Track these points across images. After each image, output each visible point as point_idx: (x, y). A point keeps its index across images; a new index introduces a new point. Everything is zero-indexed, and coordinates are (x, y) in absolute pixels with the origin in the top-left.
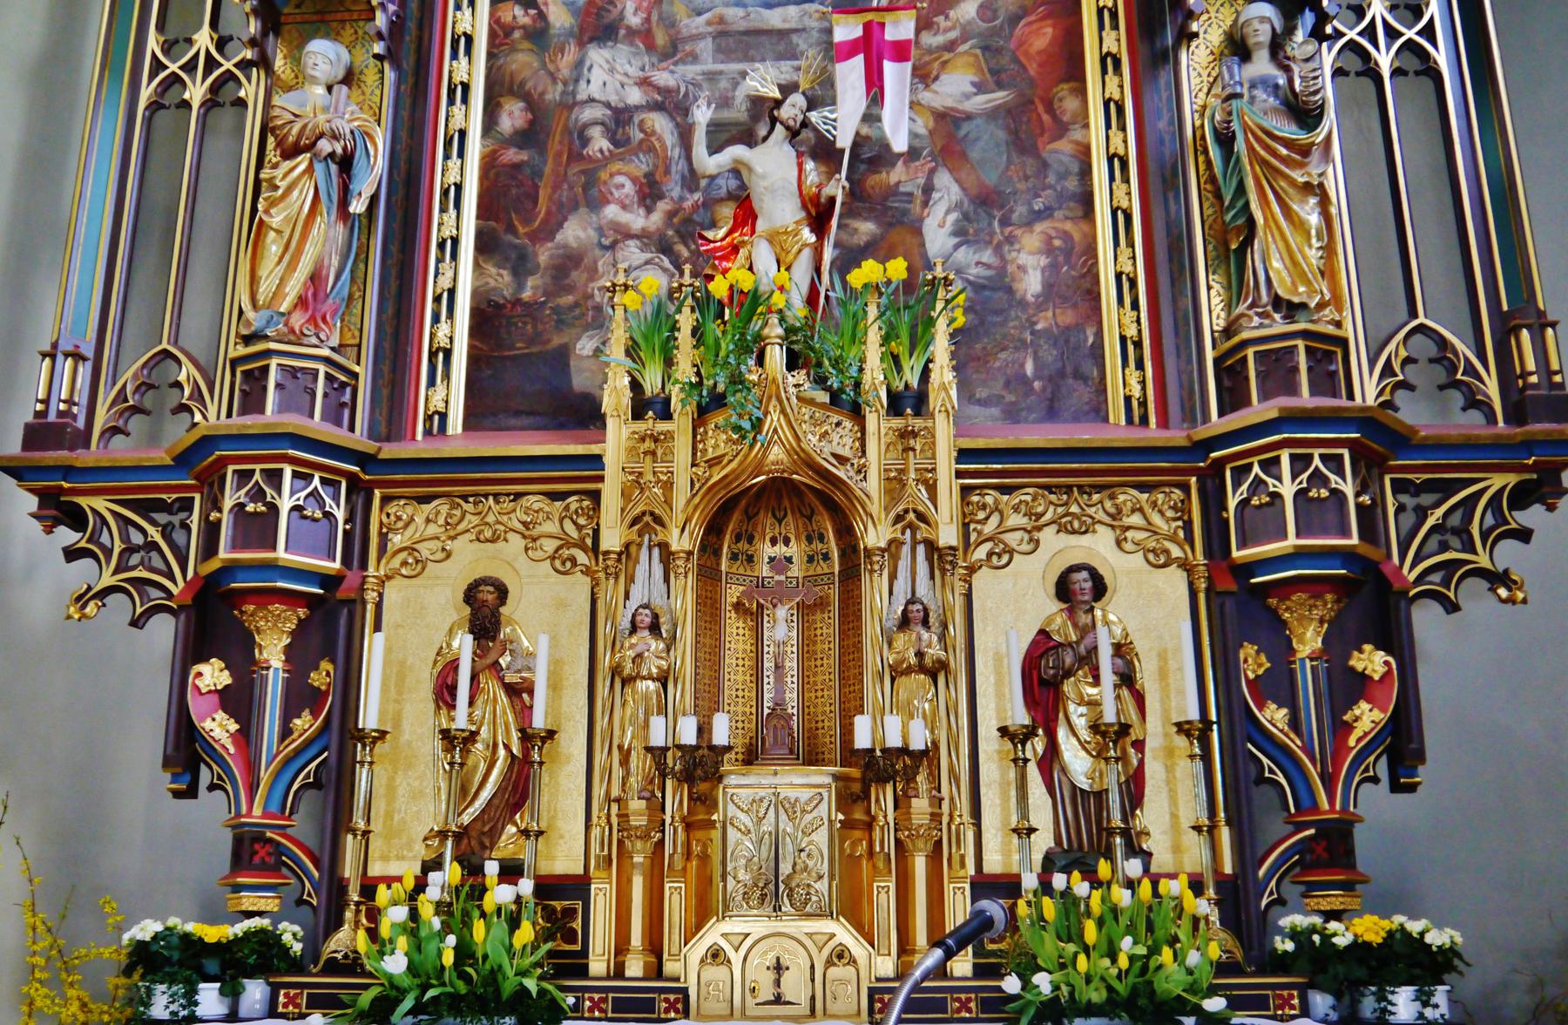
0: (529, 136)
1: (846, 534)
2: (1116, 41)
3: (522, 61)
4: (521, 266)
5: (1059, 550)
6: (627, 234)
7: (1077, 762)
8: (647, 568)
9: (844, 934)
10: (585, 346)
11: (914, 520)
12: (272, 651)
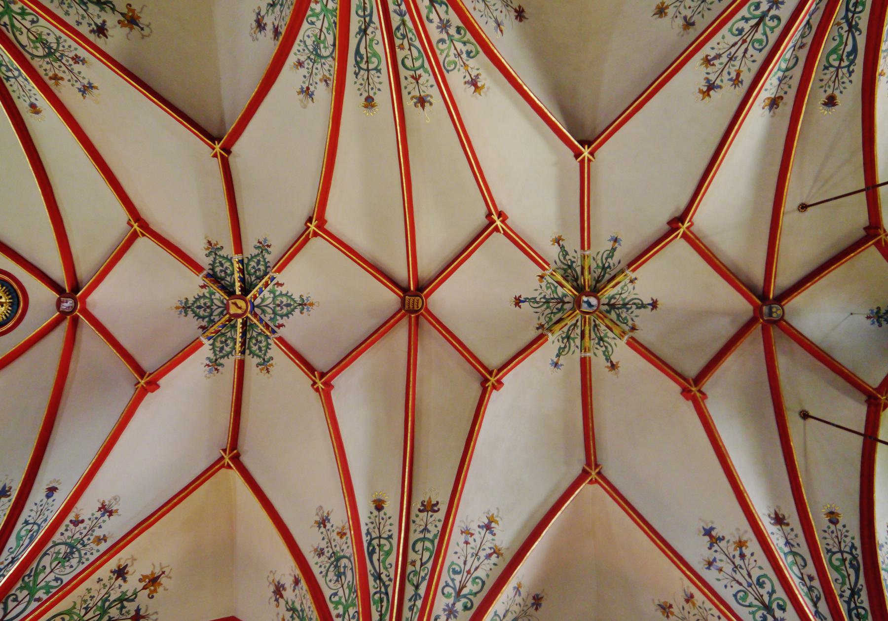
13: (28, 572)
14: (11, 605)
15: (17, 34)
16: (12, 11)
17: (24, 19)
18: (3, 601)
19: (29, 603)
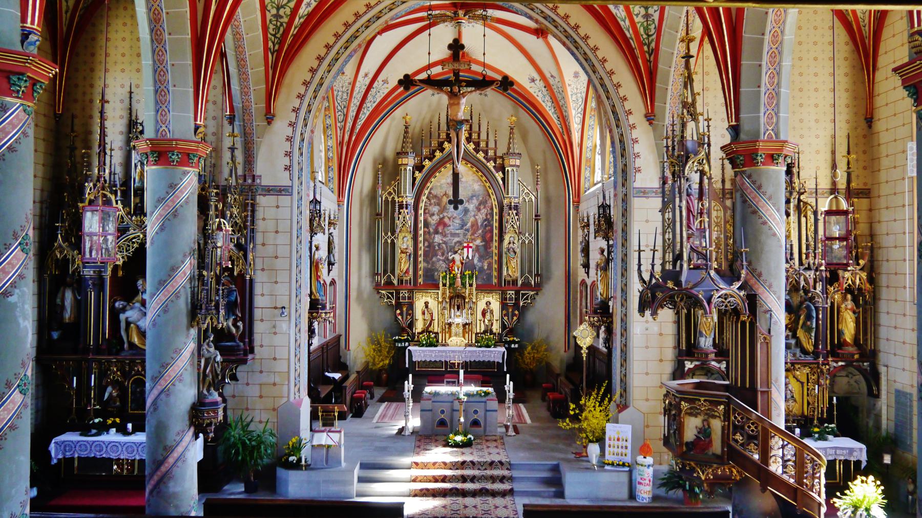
0: (429, 246)
2: (497, 239)
5: (486, 299)
6: (440, 260)
7: (486, 321)
8: (444, 303)
9: (463, 339)
10: (436, 274)
11: (471, 299)
12: (405, 309)
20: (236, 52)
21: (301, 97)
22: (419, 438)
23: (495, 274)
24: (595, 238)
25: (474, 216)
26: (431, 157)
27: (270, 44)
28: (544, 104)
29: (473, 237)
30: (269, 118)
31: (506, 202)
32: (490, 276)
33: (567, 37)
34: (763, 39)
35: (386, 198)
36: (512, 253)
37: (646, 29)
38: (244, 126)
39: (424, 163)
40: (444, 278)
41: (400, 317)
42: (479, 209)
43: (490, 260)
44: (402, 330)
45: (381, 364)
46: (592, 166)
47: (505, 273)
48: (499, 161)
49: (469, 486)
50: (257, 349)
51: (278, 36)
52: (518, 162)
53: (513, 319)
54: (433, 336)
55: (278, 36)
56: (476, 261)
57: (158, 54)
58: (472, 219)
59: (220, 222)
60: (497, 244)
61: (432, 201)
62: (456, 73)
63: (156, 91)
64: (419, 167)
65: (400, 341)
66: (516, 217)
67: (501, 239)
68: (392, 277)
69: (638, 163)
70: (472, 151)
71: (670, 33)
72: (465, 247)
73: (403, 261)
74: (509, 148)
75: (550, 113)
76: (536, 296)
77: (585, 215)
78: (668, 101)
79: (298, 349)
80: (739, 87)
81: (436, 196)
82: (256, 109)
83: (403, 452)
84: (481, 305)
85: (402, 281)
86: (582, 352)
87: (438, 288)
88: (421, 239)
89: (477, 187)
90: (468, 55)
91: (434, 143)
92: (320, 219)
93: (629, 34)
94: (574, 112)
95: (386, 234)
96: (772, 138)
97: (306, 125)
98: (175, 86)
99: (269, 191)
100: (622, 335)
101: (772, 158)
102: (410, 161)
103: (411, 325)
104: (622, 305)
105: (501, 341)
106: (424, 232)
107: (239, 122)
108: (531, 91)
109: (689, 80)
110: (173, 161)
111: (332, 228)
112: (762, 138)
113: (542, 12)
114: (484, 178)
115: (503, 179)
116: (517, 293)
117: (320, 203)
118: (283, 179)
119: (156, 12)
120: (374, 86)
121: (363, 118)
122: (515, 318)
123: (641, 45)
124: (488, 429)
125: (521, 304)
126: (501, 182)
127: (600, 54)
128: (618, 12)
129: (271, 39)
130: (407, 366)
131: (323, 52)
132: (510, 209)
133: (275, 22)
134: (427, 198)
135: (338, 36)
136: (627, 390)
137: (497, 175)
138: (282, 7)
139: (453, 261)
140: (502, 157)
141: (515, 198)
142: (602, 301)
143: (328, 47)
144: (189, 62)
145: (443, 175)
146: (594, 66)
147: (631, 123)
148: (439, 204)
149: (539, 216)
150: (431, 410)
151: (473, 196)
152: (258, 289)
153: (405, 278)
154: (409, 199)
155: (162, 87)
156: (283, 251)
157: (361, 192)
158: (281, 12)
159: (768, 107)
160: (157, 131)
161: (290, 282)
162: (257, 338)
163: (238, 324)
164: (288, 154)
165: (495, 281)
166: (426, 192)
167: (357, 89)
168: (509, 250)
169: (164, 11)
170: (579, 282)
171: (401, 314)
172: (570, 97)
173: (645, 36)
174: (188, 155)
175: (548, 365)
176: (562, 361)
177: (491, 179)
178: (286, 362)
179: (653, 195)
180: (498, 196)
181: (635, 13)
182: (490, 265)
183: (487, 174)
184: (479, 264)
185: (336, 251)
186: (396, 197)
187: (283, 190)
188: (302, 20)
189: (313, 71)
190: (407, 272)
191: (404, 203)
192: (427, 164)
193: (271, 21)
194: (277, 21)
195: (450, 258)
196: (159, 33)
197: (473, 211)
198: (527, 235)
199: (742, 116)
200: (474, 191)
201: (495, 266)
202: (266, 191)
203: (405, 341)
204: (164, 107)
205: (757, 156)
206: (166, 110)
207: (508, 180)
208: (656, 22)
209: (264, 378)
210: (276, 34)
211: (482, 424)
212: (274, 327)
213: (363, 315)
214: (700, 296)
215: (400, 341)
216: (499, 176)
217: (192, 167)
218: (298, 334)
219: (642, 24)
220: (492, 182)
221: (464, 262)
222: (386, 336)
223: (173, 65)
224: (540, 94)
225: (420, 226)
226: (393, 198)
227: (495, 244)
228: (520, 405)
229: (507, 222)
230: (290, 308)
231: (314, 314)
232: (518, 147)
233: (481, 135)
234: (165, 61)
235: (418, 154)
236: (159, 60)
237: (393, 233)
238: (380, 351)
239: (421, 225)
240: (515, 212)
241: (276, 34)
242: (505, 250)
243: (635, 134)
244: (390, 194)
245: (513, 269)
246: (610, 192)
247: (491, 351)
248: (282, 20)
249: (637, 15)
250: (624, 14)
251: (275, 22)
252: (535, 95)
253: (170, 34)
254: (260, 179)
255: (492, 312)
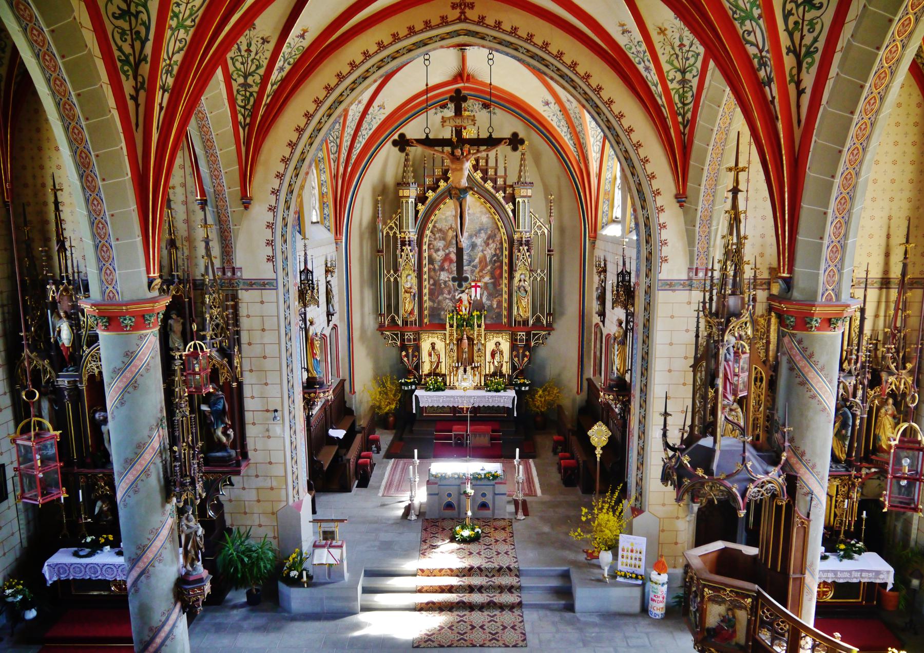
0: (434, 284)
1: (473, 342)
2: (506, 275)
3: (432, 273)
4: (433, 301)
5: (496, 340)
7: (496, 363)
8: (451, 344)
10: (442, 313)
12: (410, 351)
13: (730, 13)
14: (751, 38)
15: (195, 9)
16: (178, 22)
17: (180, 12)
18: (744, 42)
19: (758, 24)
20: (200, 132)
21: (280, 176)
22: (426, 524)
23: (505, 313)
24: (613, 308)
25: (482, 251)
26: (434, 188)
27: (240, 117)
28: (559, 130)
29: (481, 274)
30: (246, 202)
31: (516, 237)
32: (499, 315)
33: (587, 100)
34: (833, 182)
35: (388, 233)
36: (523, 292)
37: (682, 97)
38: (218, 213)
39: (427, 195)
40: (452, 318)
41: (405, 359)
42: (488, 245)
43: (499, 298)
44: (406, 372)
45: (388, 408)
46: (611, 199)
47: (515, 312)
48: (509, 190)
49: (477, 598)
50: (251, 454)
51: (249, 107)
52: (529, 192)
53: (523, 360)
54: (440, 379)
55: (249, 107)
56: (484, 300)
57: (93, 203)
58: (480, 254)
59: (195, 344)
60: (506, 282)
61: (437, 236)
62: (459, 132)
63: (96, 247)
64: (422, 199)
65: (406, 384)
66: (528, 254)
67: (511, 277)
68: (396, 318)
69: (665, 251)
70: (480, 180)
71: (710, 106)
72: (473, 287)
73: (407, 302)
74: (520, 177)
75: (566, 139)
76: (547, 336)
77: (602, 258)
78: (704, 182)
79: (294, 452)
80: (796, 233)
81: (440, 230)
82: (229, 193)
83: (407, 554)
84: (490, 346)
85: (407, 322)
86: (597, 453)
87: (445, 329)
88: (426, 276)
89: (485, 219)
90: (473, 77)
91: (438, 172)
92: (312, 292)
93: (662, 101)
94: (592, 140)
95: (389, 272)
96: (831, 299)
97: (288, 208)
98: (118, 239)
99: (251, 285)
100: (639, 437)
101: (829, 322)
102: (411, 193)
103: (417, 367)
104: (641, 406)
105: (511, 384)
106: (429, 269)
107: (212, 207)
108: (545, 115)
109: (735, 219)
110: (126, 326)
111: (329, 276)
112: (819, 299)
113: (558, 70)
114: (493, 210)
115: (514, 211)
116: (528, 334)
117: (312, 272)
118: (266, 272)
119: (84, 155)
120: (369, 112)
121: (358, 147)
122: (526, 359)
123: (674, 114)
124: (496, 511)
125: (532, 344)
126: (511, 215)
127: (626, 123)
128: (648, 75)
129: (240, 112)
130: (414, 412)
131: (302, 122)
132: (521, 244)
133: (243, 93)
134: (431, 232)
135: (318, 103)
136: (643, 494)
137: (506, 206)
138: (251, 74)
139: (460, 300)
140: (511, 186)
141: (526, 232)
142: (618, 377)
143: (309, 116)
144: (132, 206)
145: (448, 207)
146: (618, 136)
147: (658, 205)
148: (444, 239)
149: (552, 251)
150: (437, 494)
151: (480, 230)
152: (247, 391)
153: (409, 320)
154: (411, 234)
155: (103, 242)
156: (271, 350)
157: (361, 224)
158: (250, 80)
159: (830, 263)
160: (103, 293)
161: (281, 384)
162: (250, 443)
163: (228, 432)
164: (270, 243)
165: (505, 320)
166: (430, 225)
167: (350, 118)
168: (519, 288)
169: (92, 153)
170: (594, 324)
171: (407, 356)
172: (588, 123)
173: (680, 105)
174: (143, 316)
175: (560, 407)
176: (574, 400)
177: (500, 212)
178: (282, 467)
179: (681, 287)
180: (509, 229)
181: (670, 78)
182: (500, 304)
183: (496, 205)
184: (488, 303)
185: (335, 300)
186: (398, 232)
187: (267, 284)
188: (275, 87)
189: (292, 145)
190: (412, 313)
191: (407, 239)
192: (431, 195)
193: (238, 91)
194: (246, 91)
195: (457, 298)
196: (90, 179)
197: (481, 246)
198: (539, 271)
199: (797, 269)
200: (482, 224)
201: (505, 305)
202: (248, 285)
203: (411, 384)
204: (107, 265)
205: (812, 320)
206: (111, 268)
207: (519, 212)
208: (695, 90)
209: (260, 482)
210: (245, 105)
211: (491, 506)
212: (268, 430)
213: (368, 354)
214: (734, 490)
215: (406, 384)
216: (509, 207)
217: (150, 328)
218: (293, 437)
219: (677, 92)
220: (502, 215)
221: (472, 302)
222: (392, 379)
223: (112, 215)
224: (554, 118)
225: (424, 263)
226: (395, 233)
227: (505, 281)
228: (531, 461)
229: (518, 259)
230: (282, 411)
231: (312, 395)
232: (530, 175)
233: (490, 161)
234: (103, 212)
235: (421, 184)
236: (94, 210)
237: (396, 271)
238: (386, 394)
239: (426, 262)
240: (526, 248)
241: (245, 105)
242: (515, 288)
243: (663, 218)
244: (391, 228)
245: (523, 309)
246: (632, 253)
247: (501, 397)
248: (251, 90)
249: (672, 81)
250: (656, 78)
251: (243, 93)
252: (549, 119)
253: (104, 180)
254: (241, 272)
255: (501, 353)
